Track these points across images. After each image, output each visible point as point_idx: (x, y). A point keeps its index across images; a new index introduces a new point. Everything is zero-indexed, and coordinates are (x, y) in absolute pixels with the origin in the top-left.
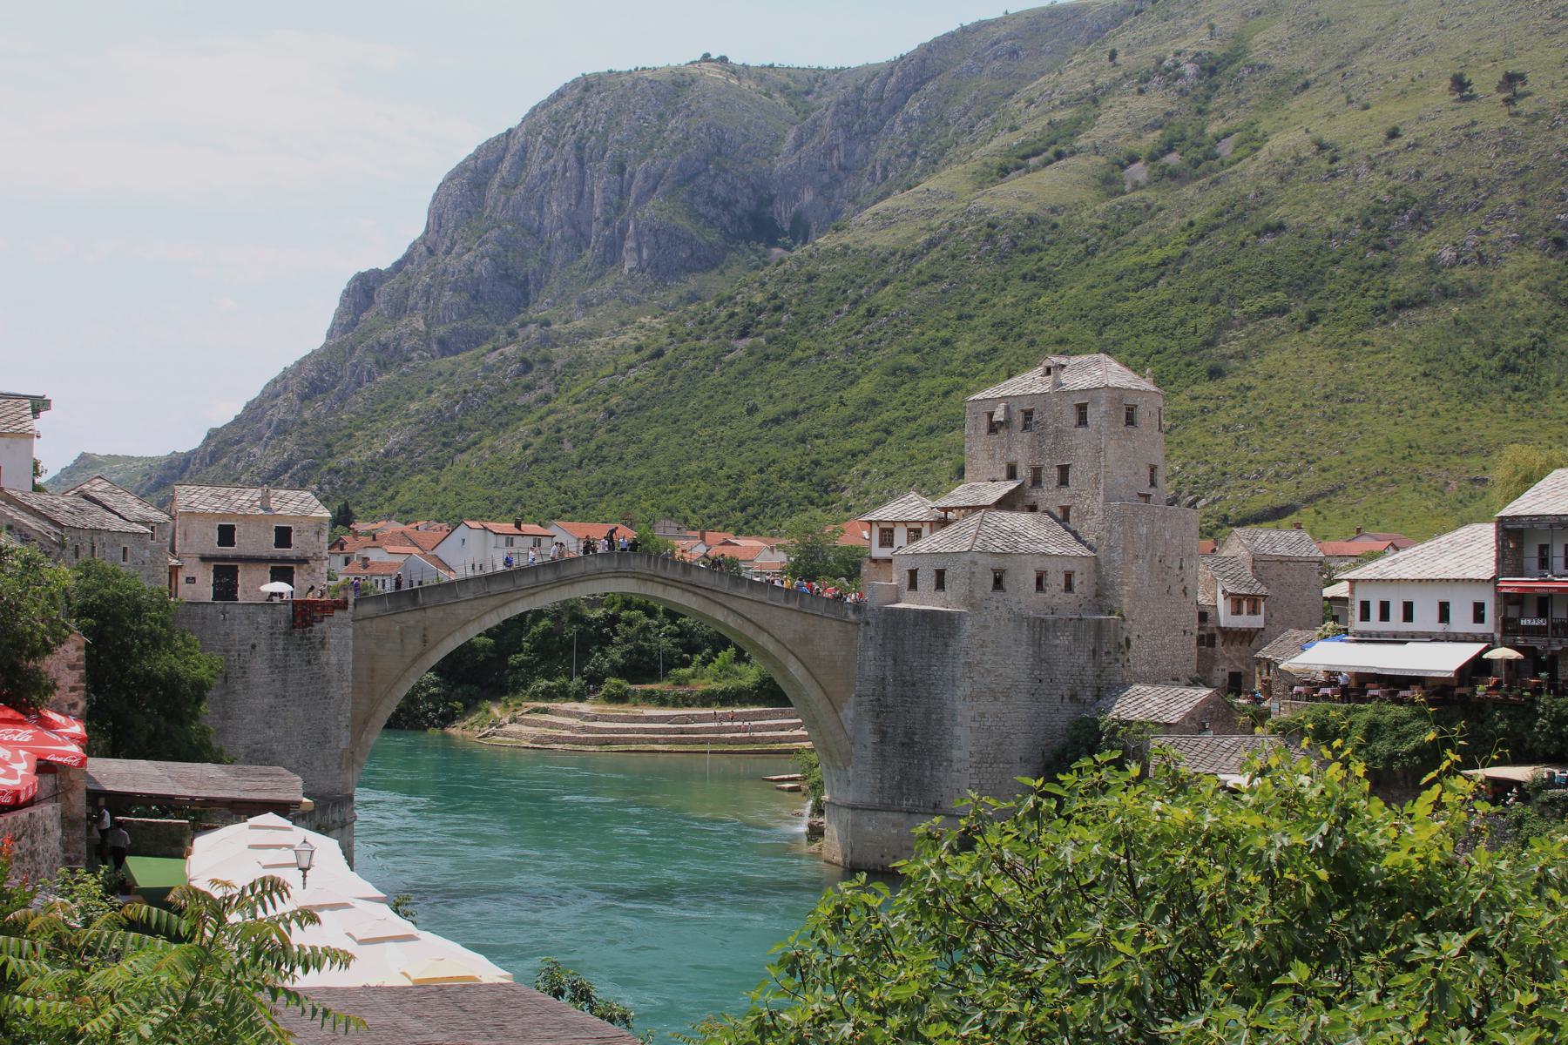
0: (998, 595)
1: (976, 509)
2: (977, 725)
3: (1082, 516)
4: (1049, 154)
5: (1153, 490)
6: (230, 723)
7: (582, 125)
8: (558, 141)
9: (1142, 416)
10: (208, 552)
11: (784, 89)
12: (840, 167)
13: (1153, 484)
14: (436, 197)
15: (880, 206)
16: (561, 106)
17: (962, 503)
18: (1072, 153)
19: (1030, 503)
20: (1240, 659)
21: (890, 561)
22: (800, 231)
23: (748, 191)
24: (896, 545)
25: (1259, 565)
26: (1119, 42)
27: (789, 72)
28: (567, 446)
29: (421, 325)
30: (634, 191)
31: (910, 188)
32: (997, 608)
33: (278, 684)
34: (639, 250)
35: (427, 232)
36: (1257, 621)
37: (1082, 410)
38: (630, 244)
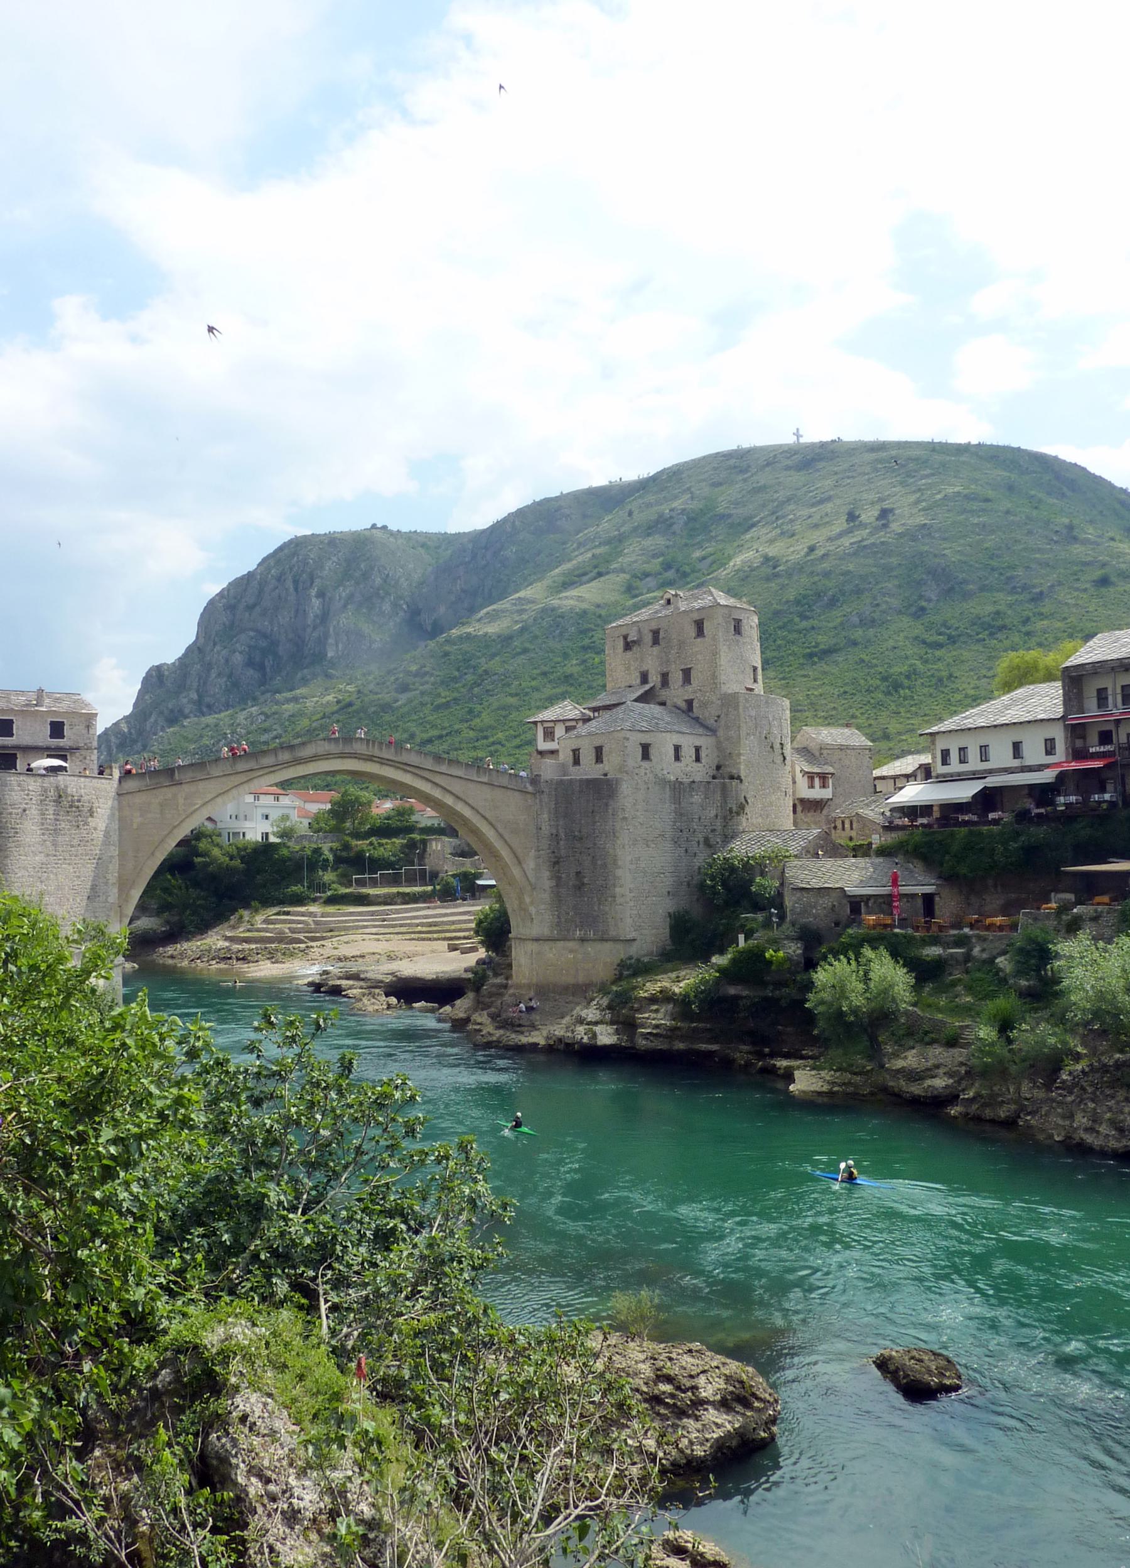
0: (645, 764)
2: (634, 866)
3: (704, 705)
9: (745, 627)
11: (423, 545)
12: (463, 591)
14: (202, 615)
18: (608, 573)
19: (662, 699)
23: (405, 606)
25: (825, 752)
29: (195, 696)
34: (337, 646)
35: (197, 637)
36: (827, 793)
37: (699, 626)
38: (331, 641)
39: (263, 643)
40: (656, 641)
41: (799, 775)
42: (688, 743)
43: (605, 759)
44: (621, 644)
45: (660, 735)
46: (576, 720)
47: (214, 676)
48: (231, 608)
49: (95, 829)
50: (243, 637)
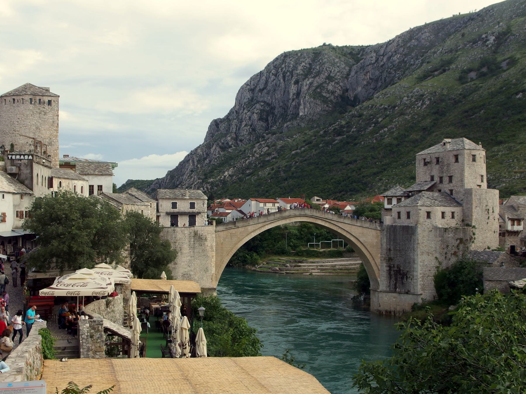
0: (428, 220)
1: (420, 191)
2: (422, 264)
4: (441, 70)
5: (482, 183)
6: (176, 266)
7: (284, 69)
8: (276, 74)
9: (478, 158)
10: (168, 211)
11: (351, 54)
13: (482, 181)
14: (238, 94)
15: (384, 91)
16: (277, 63)
17: (415, 189)
18: (449, 69)
19: (439, 188)
20: (515, 242)
21: (391, 209)
22: (356, 101)
23: (339, 88)
24: (393, 204)
25: (521, 209)
26: (465, 31)
27: (352, 48)
28: (282, 173)
30: (302, 90)
31: (393, 84)
32: (428, 224)
33: (192, 253)
34: (304, 109)
35: (235, 106)
36: (520, 228)
38: (302, 107)
39: (267, 109)
40: (438, 162)
41: (507, 219)
42: (448, 210)
43: (411, 217)
44: (422, 163)
45: (435, 208)
46: (402, 196)
47: (243, 126)
48: (252, 90)
49: (207, 246)
50: (258, 106)
